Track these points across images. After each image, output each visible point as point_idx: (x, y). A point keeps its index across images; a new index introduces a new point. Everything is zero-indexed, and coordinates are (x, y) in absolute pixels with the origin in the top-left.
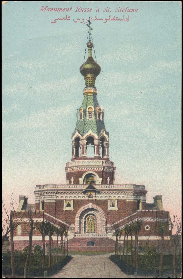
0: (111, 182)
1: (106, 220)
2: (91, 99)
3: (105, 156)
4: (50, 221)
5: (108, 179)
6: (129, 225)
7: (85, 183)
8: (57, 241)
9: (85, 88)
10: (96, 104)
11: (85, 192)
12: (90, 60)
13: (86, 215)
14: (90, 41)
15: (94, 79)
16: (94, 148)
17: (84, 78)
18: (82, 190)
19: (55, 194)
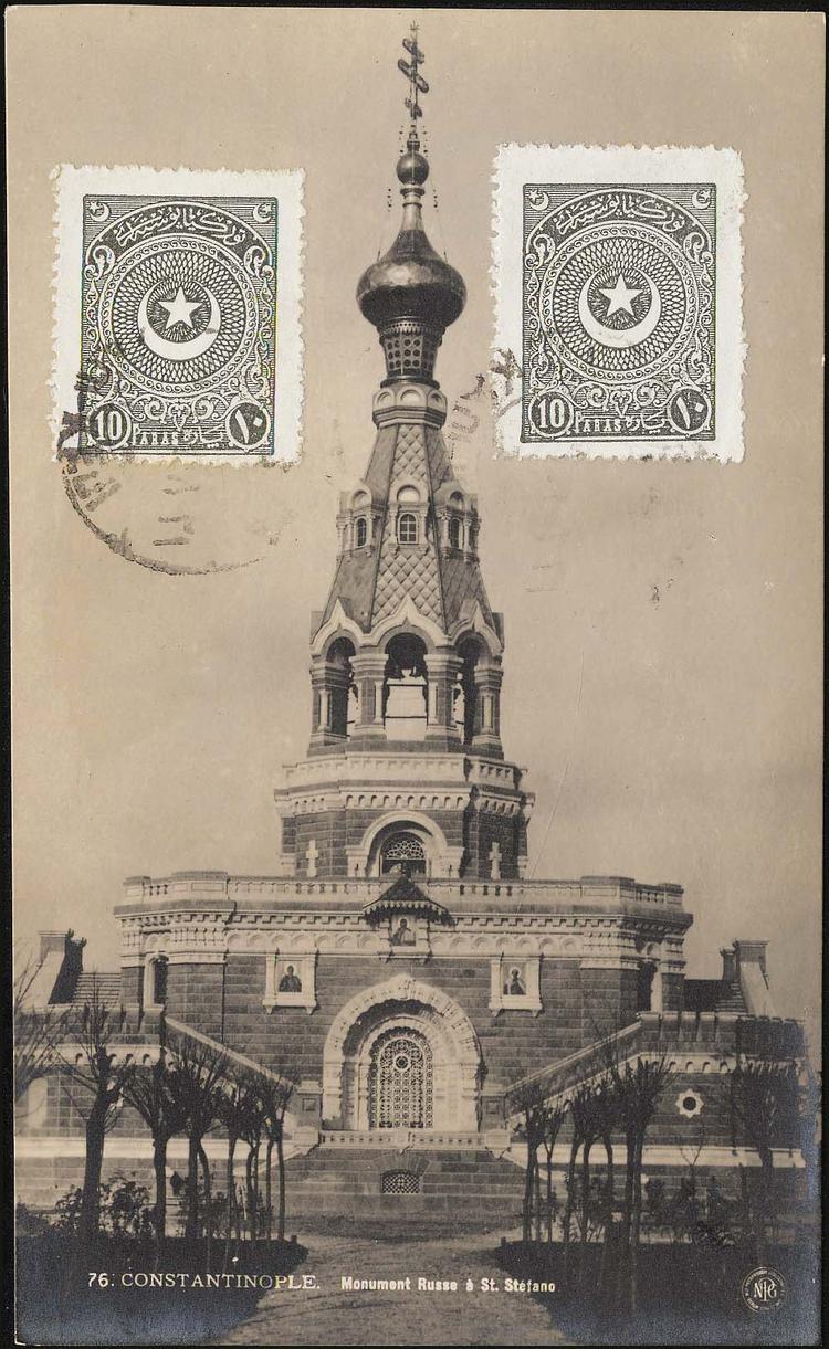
0: (510, 871)
1: (478, 1060)
2: (416, 445)
3: (478, 733)
4: (195, 1061)
5: (495, 855)
6: (598, 1092)
7: (375, 872)
8: (230, 1164)
9: (383, 385)
10: (439, 472)
11: (375, 918)
12: (413, 246)
13: (382, 1030)
14: (413, 147)
15: (433, 341)
16: (426, 695)
17: (376, 336)
18: (357, 906)
19: (224, 925)
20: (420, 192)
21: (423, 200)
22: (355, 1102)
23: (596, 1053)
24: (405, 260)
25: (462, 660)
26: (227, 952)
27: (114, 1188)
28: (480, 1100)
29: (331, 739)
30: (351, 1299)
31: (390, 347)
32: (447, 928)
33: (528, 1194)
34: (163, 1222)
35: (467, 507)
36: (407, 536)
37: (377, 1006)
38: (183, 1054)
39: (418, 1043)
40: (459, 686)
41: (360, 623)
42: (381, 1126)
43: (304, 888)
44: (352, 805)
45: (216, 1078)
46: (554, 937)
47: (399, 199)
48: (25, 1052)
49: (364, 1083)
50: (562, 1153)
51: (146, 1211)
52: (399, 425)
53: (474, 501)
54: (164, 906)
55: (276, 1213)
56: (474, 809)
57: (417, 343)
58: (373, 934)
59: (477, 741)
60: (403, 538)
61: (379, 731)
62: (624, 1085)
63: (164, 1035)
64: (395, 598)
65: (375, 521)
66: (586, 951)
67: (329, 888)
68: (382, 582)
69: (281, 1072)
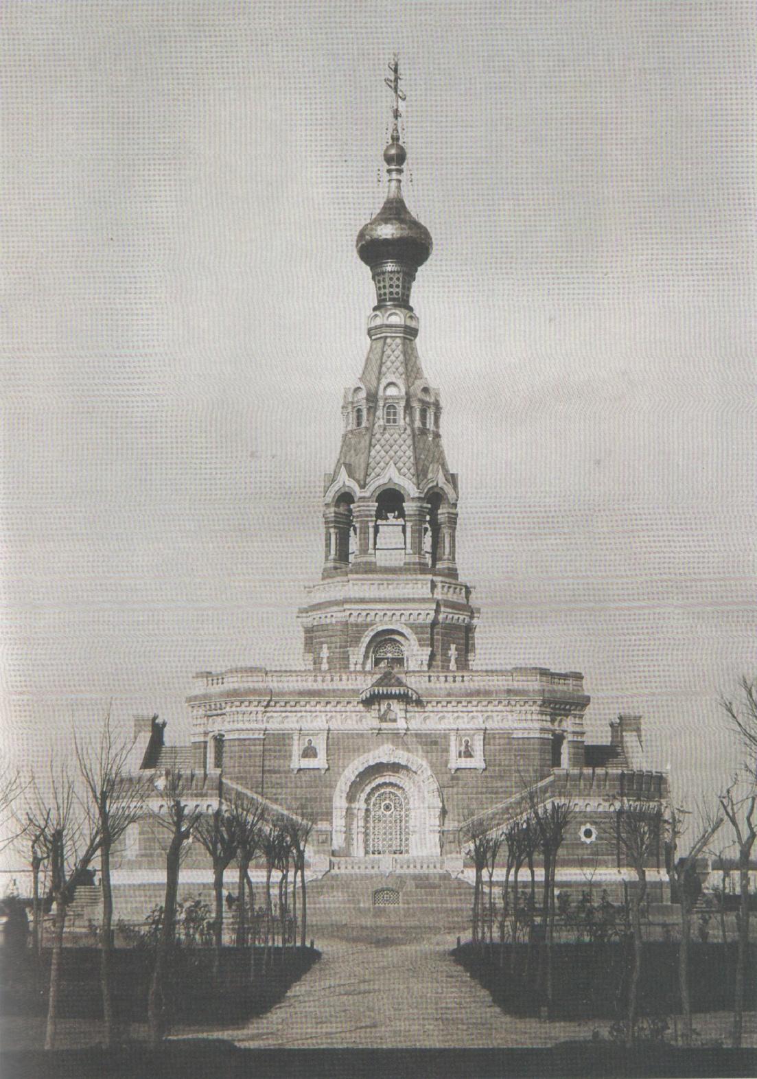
0: (463, 664)
1: (441, 805)
2: (397, 353)
3: (441, 559)
4: (243, 809)
5: (453, 652)
6: (525, 826)
7: (368, 667)
8: (268, 886)
9: (375, 309)
10: (411, 368)
11: (371, 701)
12: (395, 210)
13: (373, 785)
14: (396, 139)
15: (409, 277)
16: (404, 531)
17: (370, 274)
18: (356, 692)
19: (263, 709)
20: (400, 171)
21: (403, 177)
22: (354, 836)
23: (522, 798)
24: (390, 219)
25: (429, 506)
26: (266, 730)
27: (187, 905)
28: (442, 833)
29: (338, 565)
30: (352, 988)
31: (379, 282)
32: (419, 709)
33: (476, 904)
34: (220, 929)
35: (432, 400)
36: (391, 419)
37: (370, 767)
38: (235, 804)
39: (399, 793)
40: (427, 525)
41: (358, 481)
42: (373, 853)
43: (319, 679)
44: (352, 620)
45: (258, 821)
46: (495, 714)
47: (385, 177)
48: (124, 805)
49: (361, 823)
50: (499, 874)
51: (208, 923)
52: (386, 337)
53: (437, 394)
54: (221, 695)
55: (299, 923)
56: (450, 527)
57: (398, 279)
58: (368, 714)
59: (439, 566)
60: (388, 421)
61: (372, 559)
62: (543, 821)
63: (220, 789)
64: (382, 464)
65: (369, 409)
66: (516, 725)
67: (337, 678)
68: (373, 453)
69: (303, 815)
